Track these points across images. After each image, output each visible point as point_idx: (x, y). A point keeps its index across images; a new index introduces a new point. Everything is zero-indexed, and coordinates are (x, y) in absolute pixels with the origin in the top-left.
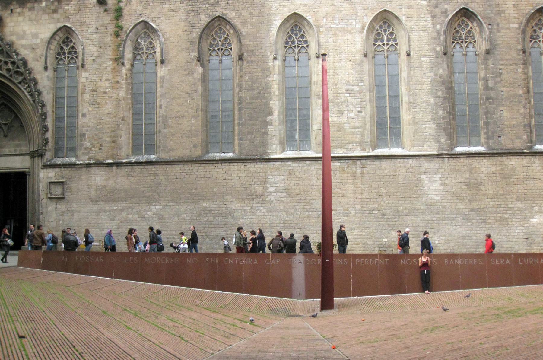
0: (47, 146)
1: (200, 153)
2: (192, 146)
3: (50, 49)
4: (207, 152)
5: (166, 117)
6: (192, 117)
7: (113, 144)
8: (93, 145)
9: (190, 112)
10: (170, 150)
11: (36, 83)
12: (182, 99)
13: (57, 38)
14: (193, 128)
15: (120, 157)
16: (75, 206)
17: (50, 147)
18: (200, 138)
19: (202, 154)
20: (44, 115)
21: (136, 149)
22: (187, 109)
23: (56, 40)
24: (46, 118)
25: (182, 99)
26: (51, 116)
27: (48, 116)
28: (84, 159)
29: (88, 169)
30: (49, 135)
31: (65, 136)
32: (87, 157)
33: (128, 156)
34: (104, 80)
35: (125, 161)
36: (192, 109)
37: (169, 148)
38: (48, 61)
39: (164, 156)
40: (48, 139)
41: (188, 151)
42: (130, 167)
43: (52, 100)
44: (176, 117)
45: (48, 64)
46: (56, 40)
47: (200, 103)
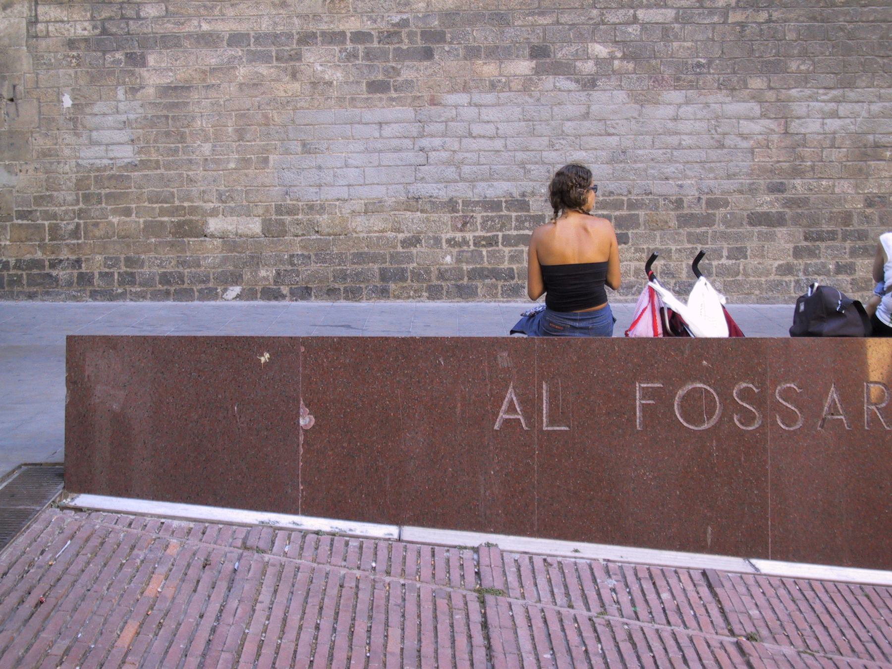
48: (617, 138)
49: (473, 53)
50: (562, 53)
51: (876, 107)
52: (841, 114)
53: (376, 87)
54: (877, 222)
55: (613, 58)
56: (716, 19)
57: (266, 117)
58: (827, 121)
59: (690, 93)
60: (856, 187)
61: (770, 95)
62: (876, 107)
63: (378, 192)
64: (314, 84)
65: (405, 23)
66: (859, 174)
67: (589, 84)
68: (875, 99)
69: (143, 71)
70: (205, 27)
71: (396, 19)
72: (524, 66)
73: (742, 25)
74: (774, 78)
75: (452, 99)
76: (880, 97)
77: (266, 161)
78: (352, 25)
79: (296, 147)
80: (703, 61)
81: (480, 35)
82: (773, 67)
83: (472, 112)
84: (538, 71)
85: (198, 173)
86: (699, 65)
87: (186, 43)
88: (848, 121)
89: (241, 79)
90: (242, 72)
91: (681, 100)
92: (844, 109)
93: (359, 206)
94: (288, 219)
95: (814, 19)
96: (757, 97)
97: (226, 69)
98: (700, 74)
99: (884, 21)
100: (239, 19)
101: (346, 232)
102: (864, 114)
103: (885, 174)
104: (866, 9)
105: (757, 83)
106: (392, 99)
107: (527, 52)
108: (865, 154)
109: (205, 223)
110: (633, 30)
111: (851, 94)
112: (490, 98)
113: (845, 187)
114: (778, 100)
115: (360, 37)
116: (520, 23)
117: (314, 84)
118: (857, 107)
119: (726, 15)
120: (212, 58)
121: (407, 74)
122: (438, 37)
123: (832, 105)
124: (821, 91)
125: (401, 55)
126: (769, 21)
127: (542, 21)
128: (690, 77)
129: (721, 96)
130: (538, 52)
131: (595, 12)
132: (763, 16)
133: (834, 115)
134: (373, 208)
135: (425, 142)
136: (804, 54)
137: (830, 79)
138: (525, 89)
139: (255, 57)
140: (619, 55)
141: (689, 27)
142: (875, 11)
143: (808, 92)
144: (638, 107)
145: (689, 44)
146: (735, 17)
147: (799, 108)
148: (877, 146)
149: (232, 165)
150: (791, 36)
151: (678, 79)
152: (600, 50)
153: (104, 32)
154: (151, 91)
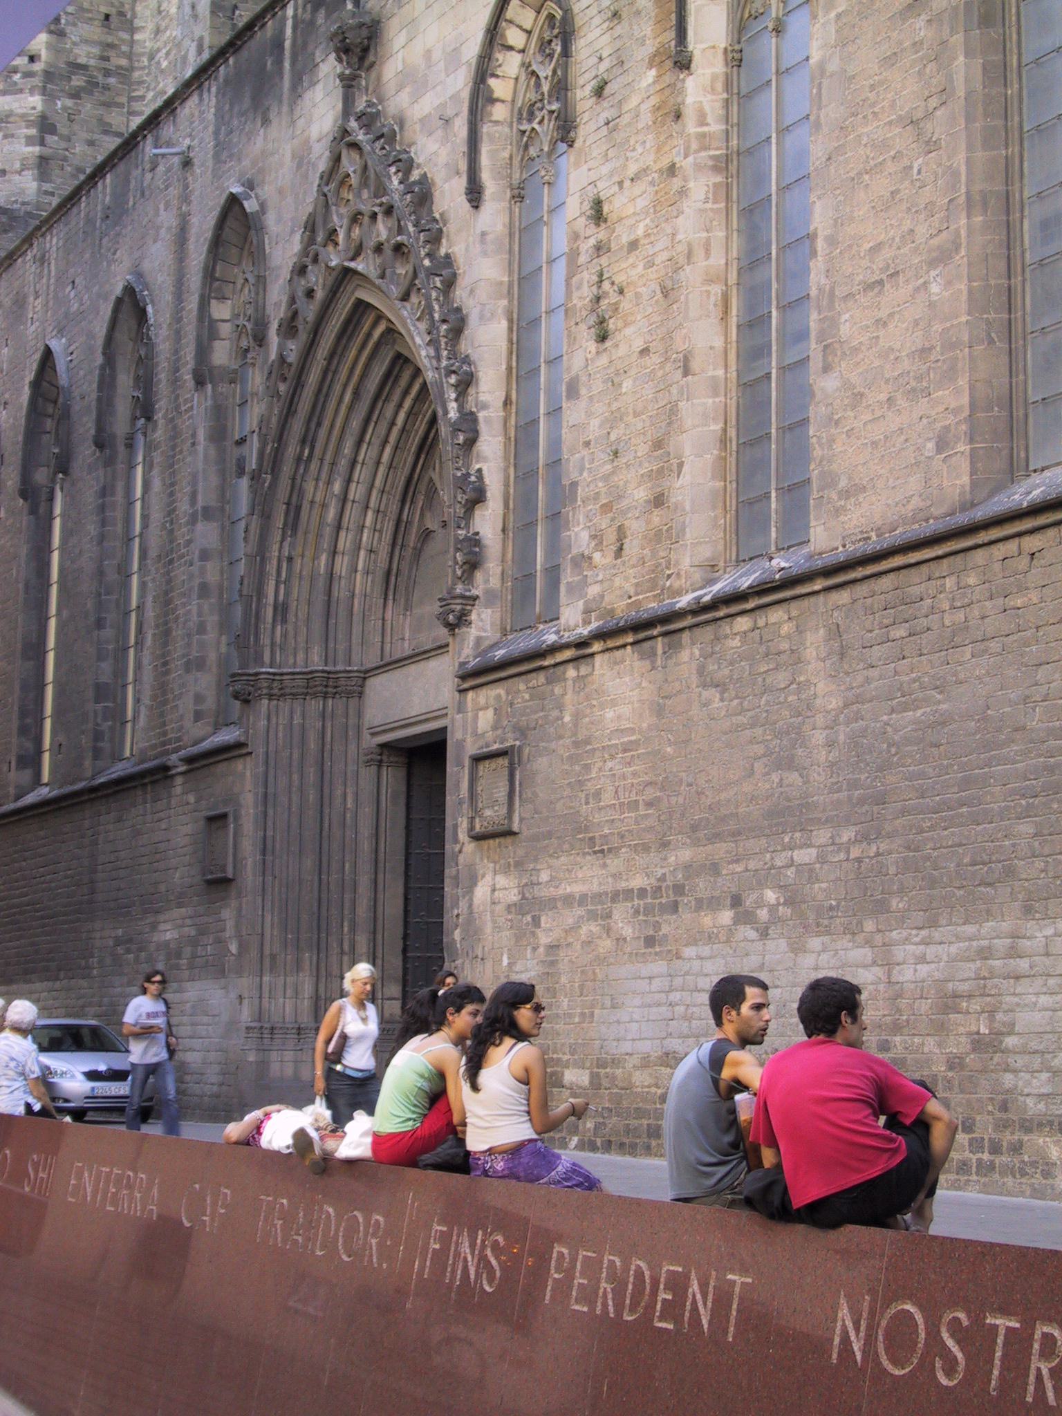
0: (479, 576)
1: (966, 479)
2: (930, 445)
3: (492, 101)
4: (1016, 470)
5: (832, 294)
6: (932, 264)
7: (657, 518)
8: (597, 537)
9: (922, 231)
10: (846, 494)
11: (450, 284)
12: (891, 167)
13: (514, 37)
14: (937, 327)
15: (677, 584)
16: (544, 877)
17: (495, 582)
18: (963, 382)
19: (974, 485)
20: (469, 425)
21: (745, 519)
22: (907, 224)
23: (511, 48)
24: (471, 442)
25: (891, 167)
26: (498, 426)
27: (483, 427)
28: (573, 619)
29: (584, 670)
30: (488, 523)
31: (541, 513)
32: (581, 603)
33: (711, 570)
34: (627, 183)
35: (683, 602)
36: (930, 207)
37: (843, 483)
38: (485, 160)
39: (826, 537)
40: (475, 541)
41: (914, 483)
42: (707, 633)
43: (503, 345)
44: (869, 287)
45: (486, 177)
46: (511, 48)
47: (960, 160)
48: (779, 990)
49: (700, 905)
50: (749, 902)
51: (953, 949)
52: (928, 958)
53: (650, 941)
54: (956, 1090)
55: (779, 904)
56: (842, 856)
57: (594, 973)
58: (919, 967)
59: (826, 939)
60: (939, 1045)
61: (878, 939)
62: (953, 949)
63: (645, 1047)
64: (618, 940)
65: (663, 878)
66: (940, 1029)
67: (764, 934)
68: (954, 939)
69: (538, 931)
70: (568, 890)
71: (660, 872)
72: (726, 916)
73: (859, 860)
74: (882, 918)
75: (689, 952)
76: (959, 938)
77: (592, 1014)
78: (638, 882)
79: (608, 1003)
80: (834, 903)
81: (703, 886)
82: (881, 907)
83: (696, 964)
84: (737, 921)
85: (560, 1027)
86: (831, 908)
87: (559, 904)
88: (933, 966)
89: (583, 937)
90: (584, 930)
91: (819, 948)
92: (931, 951)
93: (635, 1060)
94: (603, 1071)
95: (908, 848)
96: (868, 943)
97: (575, 928)
98: (832, 917)
99: (960, 845)
100: (584, 881)
101: (629, 1087)
102: (945, 958)
103: (962, 1030)
104: (946, 832)
105: (869, 926)
106: (656, 954)
107: (728, 901)
108: (946, 1006)
109: (563, 1074)
110: (790, 872)
111: (937, 935)
112: (706, 951)
113: (930, 1044)
114: (884, 945)
115: (642, 892)
116: (724, 872)
117: (618, 940)
118: (940, 948)
119: (848, 852)
120: (570, 916)
121: (665, 929)
122: (679, 889)
123: (922, 947)
124: (914, 932)
125: (663, 909)
126: (878, 854)
127: (739, 868)
128: (826, 922)
129: (845, 942)
130: (736, 901)
131: (768, 856)
132: (874, 848)
133: (922, 959)
134: (646, 1063)
135: (675, 997)
136: (902, 891)
137: (919, 917)
138: (728, 941)
139: (593, 916)
140: (782, 900)
141: (825, 867)
142: (953, 834)
143: (905, 933)
144: (792, 955)
145: (824, 885)
146: (855, 852)
147: (899, 953)
148: (955, 996)
149: (577, 1020)
150: (892, 870)
151: (818, 925)
152: (771, 896)
153: (524, 898)
154: (541, 950)
